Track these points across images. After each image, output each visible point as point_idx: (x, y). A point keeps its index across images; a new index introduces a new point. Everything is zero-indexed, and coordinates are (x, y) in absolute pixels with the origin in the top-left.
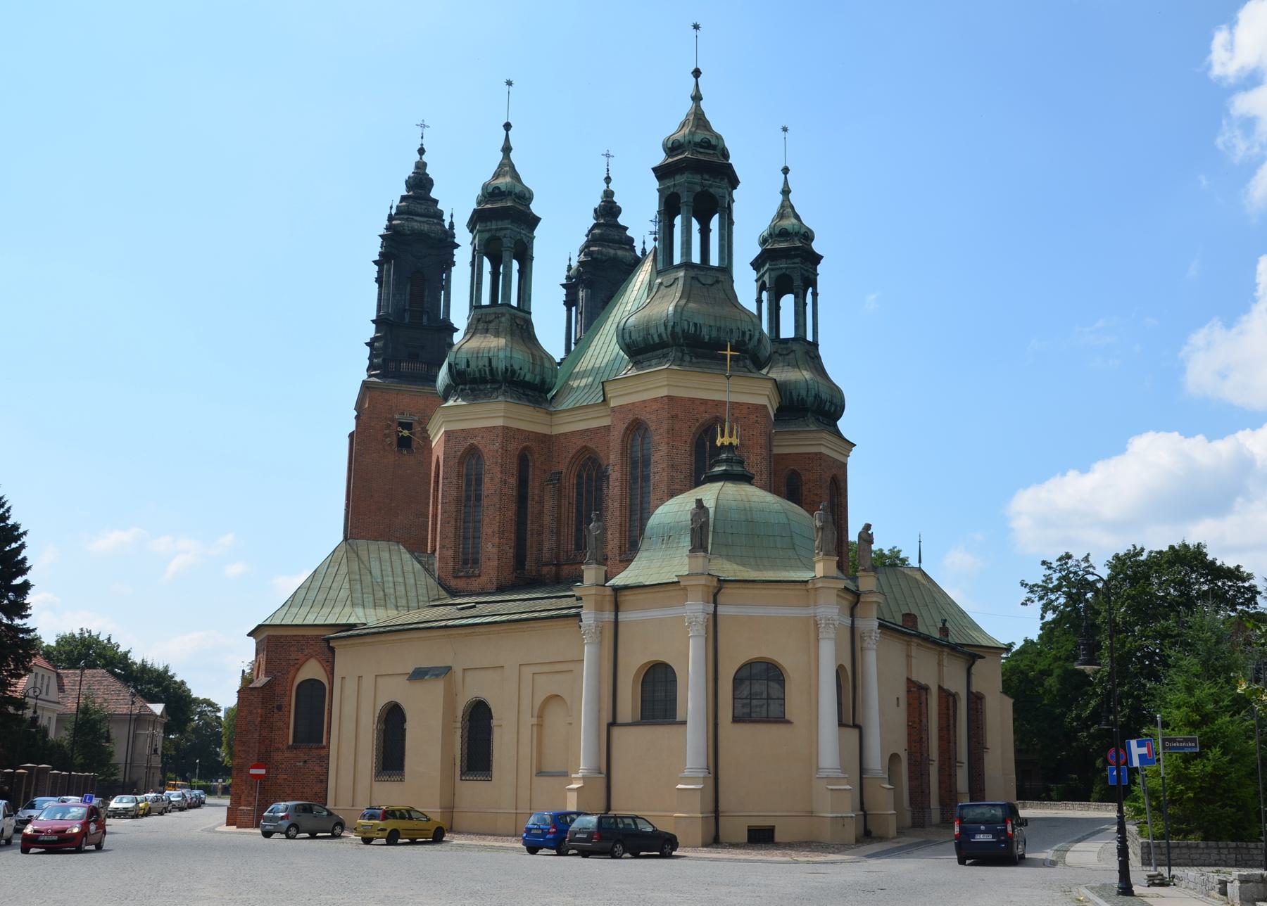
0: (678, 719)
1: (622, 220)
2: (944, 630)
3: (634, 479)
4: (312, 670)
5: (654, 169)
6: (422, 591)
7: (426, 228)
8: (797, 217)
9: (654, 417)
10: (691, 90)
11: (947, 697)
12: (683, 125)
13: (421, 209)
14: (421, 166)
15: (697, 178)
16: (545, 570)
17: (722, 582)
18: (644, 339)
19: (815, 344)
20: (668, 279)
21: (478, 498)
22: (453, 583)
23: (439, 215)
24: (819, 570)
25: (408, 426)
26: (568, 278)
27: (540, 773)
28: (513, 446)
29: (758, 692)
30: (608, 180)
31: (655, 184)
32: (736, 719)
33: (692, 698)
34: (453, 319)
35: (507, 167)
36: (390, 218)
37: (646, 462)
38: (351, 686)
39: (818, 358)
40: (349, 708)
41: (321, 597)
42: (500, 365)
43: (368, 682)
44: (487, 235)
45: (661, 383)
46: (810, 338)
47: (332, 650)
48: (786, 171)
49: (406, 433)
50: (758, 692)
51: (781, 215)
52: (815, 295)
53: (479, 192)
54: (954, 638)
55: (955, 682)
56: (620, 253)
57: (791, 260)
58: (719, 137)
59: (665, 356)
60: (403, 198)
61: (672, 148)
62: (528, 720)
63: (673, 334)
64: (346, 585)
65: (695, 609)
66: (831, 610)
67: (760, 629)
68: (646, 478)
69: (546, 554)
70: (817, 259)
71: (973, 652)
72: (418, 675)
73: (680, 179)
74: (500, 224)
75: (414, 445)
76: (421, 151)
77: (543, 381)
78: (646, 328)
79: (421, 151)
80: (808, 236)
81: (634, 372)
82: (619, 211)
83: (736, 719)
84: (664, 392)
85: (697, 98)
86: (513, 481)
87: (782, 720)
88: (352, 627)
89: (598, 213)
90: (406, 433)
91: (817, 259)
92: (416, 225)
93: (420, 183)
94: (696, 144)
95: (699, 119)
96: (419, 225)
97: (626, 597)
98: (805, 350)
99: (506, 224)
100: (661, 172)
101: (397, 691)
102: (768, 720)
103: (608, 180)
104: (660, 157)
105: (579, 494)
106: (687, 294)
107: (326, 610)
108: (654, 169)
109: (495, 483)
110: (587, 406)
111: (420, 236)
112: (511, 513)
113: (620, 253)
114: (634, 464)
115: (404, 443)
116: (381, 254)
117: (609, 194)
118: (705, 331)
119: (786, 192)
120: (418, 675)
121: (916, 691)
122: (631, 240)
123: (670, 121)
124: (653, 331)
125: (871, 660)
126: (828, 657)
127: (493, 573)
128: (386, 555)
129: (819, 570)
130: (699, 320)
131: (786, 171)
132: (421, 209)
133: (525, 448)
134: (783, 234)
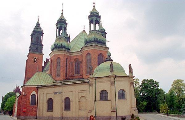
0: (109, 99)
4: (34, 93)
6: (51, 80)
7: (39, 31)
9: (91, 53)
13: (38, 28)
14: (38, 22)
15: (96, 18)
16: (70, 77)
18: (89, 41)
21: (60, 66)
22: (56, 79)
23: (41, 29)
27: (80, 110)
28: (66, 58)
34: (43, 44)
35: (62, 16)
36: (34, 29)
38: (42, 94)
40: (41, 99)
41: (35, 80)
42: (63, 45)
43: (45, 95)
44: (60, 25)
47: (38, 89)
49: (36, 60)
53: (58, 19)
58: (98, 12)
59: (93, 43)
60: (36, 26)
61: (91, 13)
62: (78, 100)
63: (94, 40)
64: (39, 79)
69: (70, 75)
72: (56, 93)
73: (93, 17)
74: (62, 24)
76: (38, 20)
77: (69, 48)
79: (38, 20)
80: (105, 30)
86: (65, 63)
88: (41, 85)
90: (36, 60)
91: (106, 34)
92: (38, 30)
93: (38, 25)
94: (95, 13)
99: (63, 24)
101: (52, 96)
105: (75, 65)
107: (36, 83)
109: (63, 63)
110: (77, 52)
111: (38, 32)
112: (65, 68)
118: (99, 40)
120: (56, 93)
123: (91, 9)
124: (91, 39)
127: (62, 78)
128: (44, 74)
130: (98, 38)
132: (38, 28)
133: (67, 58)
134: (102, 30)
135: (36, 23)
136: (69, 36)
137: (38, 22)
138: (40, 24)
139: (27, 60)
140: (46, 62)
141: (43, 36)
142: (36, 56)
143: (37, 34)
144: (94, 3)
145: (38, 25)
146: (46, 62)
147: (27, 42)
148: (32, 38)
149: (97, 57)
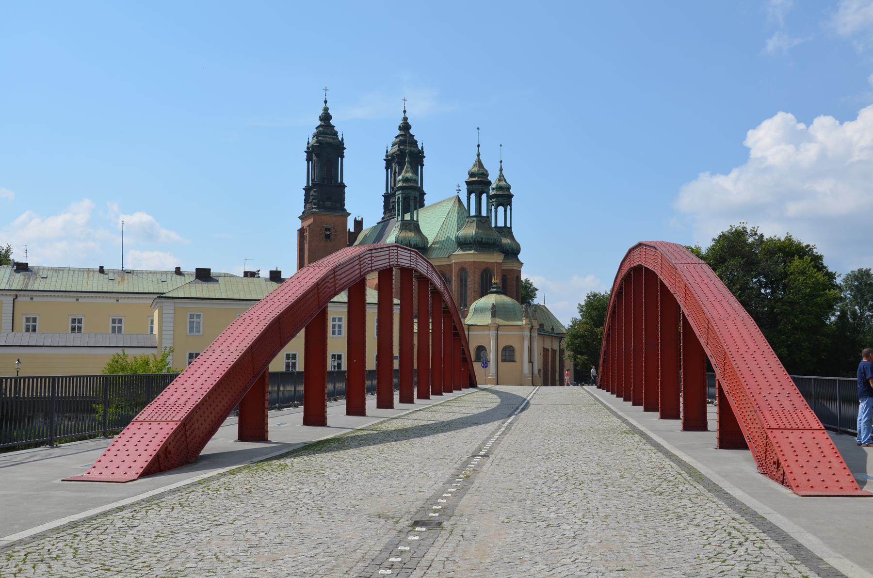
1: (411, 131)
2: (553, 329)
3: (461, 286)
5: (466, 182)
7: (332, 141)
8: (505, 181)
10: (476, 152)
11: (554, 351)
12: (475, 165)
14: (326, 109)
15: (480, 187)
17: (499, 326)
19: (511, 228)
20: (471, 220)
23: (336, 133)
24: (524, 322)
25: (327, 229)
26: (387, 156)
29: (508, 354)
30: (405, 112)
31: (466, 186)
32: (503, 361)
33: (492, 357)
34: (345, 182)
37: (466, 281)
39: (511, 233)
42: (413, 243)
45: (469, 256)
46: (508, 225)
48: (501, 162)
50: (508, 354)
51: (500, 180)
52: (511, 209)
54: (556, 331)
55: (556, 347)
56: (412, 149)
57: (504, 198)
58: (486, 171)
60: (320, 126)
61: (472, 175)
65: (492, 333)
66: (527, 333)
67: (509, 338)
68: (466, 286)
70: (512, 196)
71: (560, 337)
75: (332, 237)
76: (326, 102)
78: (465, 238)
79: (326, 102)
80: (509, 188)
81: (462, 252)
82: (410, 127)
83: (503, 361)
84: (472, 260)
85: (479, 155)
87: (514, 361)
89: (400, 128)
91: (512, 196)
92: (328, 140)
93: (326, 117)
95: (479, 164)
96: (329, 139)
97: (471, 328)
98: (507, 231)
100: (468, 183)
102: (510, 361)
103: (405, 112)
104: (466, 177)
106: (478, 227)
108: (466, 182)
111: (329, 145)
113: (412, 149)
114: (461, 281)
115: (328, 237)
116: (308, 148)
117: (405, 119)
119: (501, 170)
121: (545, 351)
122: (416, 142)
123: (469, 165)
125: (535, 344)
126: (526, 344)
129: (524, 322)
131: (501, 162)
132: (329, 131)
135: (320, 112)
136: (420, 148)
137: (326, 109)
138: (331, 117)
139: (301, 232)
140: (352, 230)
141: (342, 157)
142: (329, 219)
143: (326, 151)
144: (479, 146)
145: (326, 117)
146: (352, 230)
147: (298, 174)
148: (309, 159)
149: (478, 277)
